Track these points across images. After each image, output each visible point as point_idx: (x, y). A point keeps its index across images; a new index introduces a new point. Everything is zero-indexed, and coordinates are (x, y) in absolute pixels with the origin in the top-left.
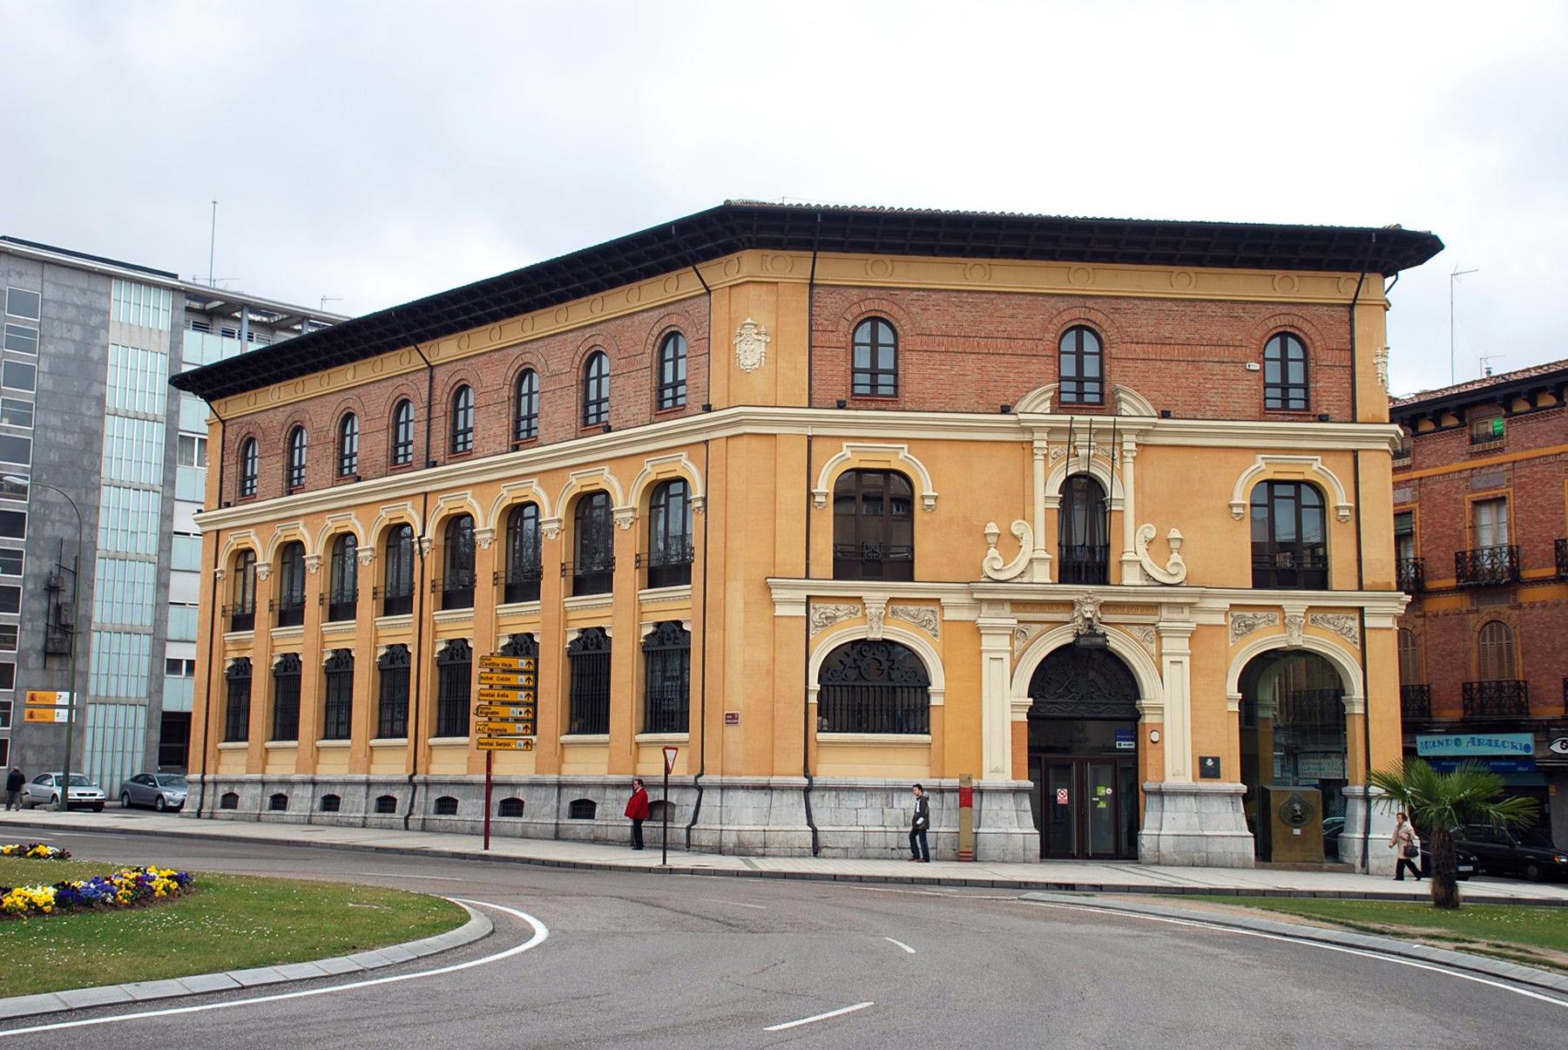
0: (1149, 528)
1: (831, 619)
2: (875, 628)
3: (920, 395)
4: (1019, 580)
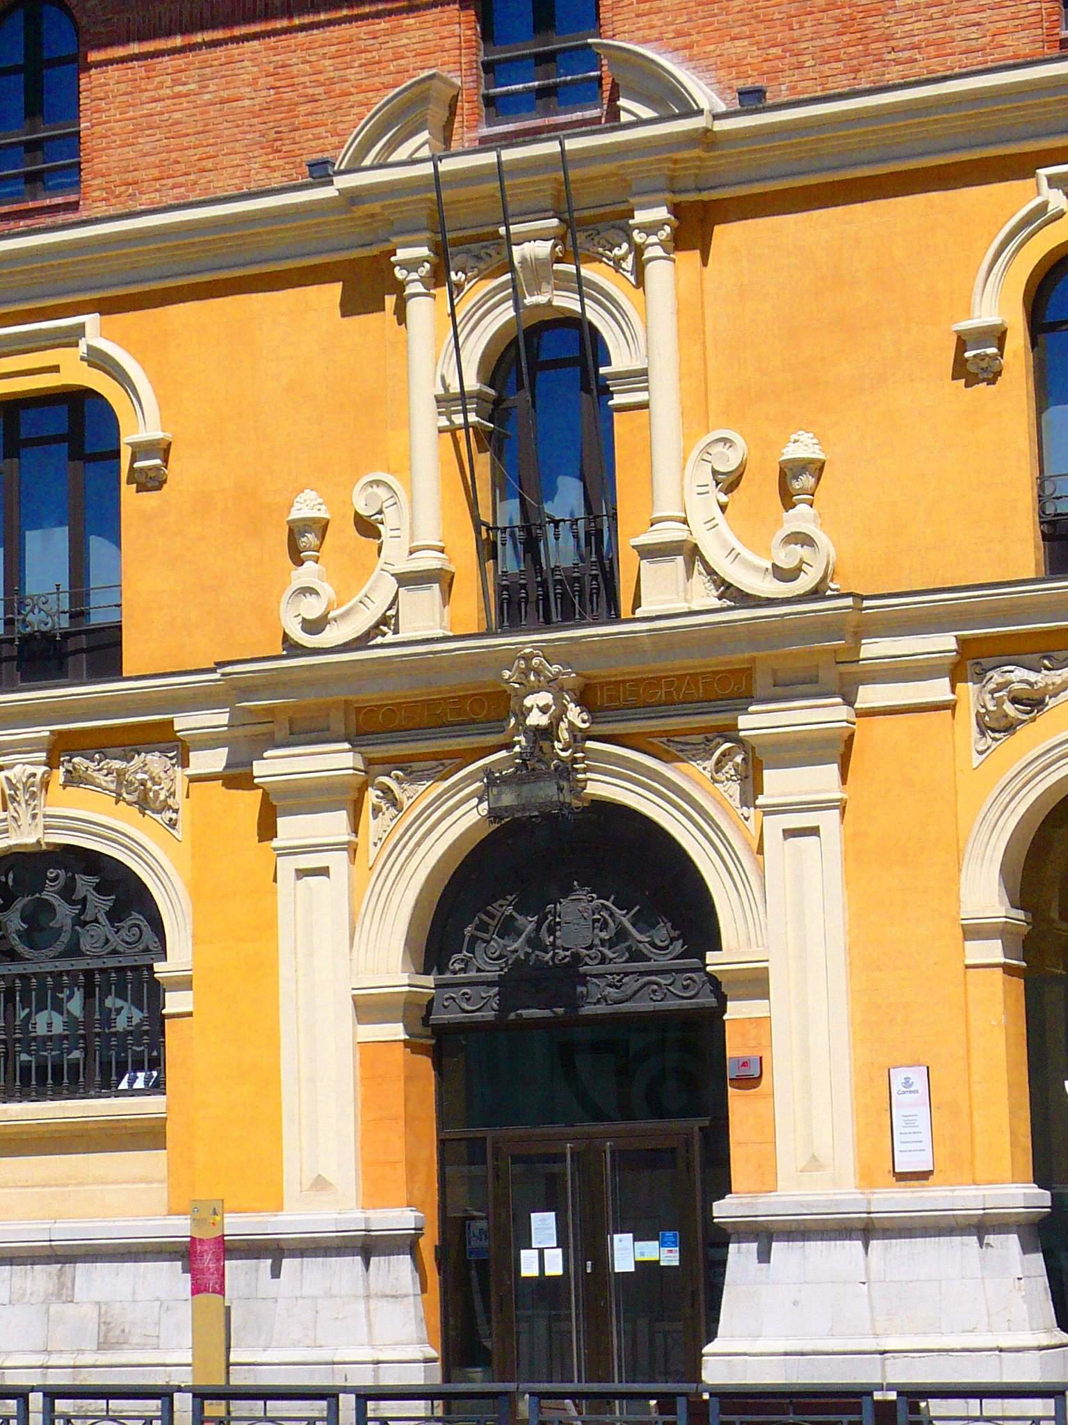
0: (725, 440)
2: (25, 819)
3: (129, 177)
4: (379, 640)
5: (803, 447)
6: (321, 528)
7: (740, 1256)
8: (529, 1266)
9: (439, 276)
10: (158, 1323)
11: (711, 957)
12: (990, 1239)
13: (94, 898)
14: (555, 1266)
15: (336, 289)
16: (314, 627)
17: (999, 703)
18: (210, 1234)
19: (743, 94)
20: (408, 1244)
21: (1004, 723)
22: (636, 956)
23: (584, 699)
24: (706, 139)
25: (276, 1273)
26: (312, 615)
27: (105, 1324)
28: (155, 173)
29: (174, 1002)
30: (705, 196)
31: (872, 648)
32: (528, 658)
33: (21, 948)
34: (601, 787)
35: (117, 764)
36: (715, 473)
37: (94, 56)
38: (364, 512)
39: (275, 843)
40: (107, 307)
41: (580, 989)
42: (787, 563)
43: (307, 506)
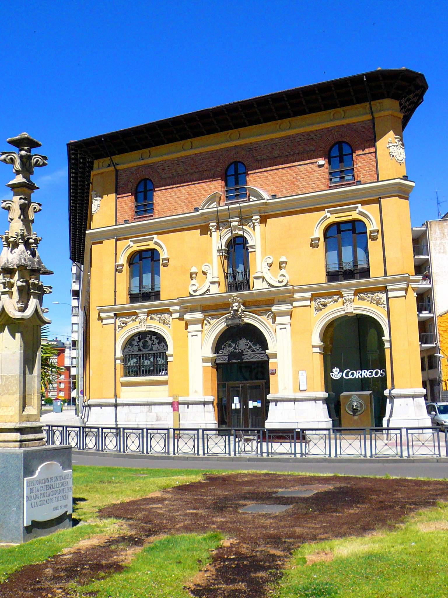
1: (126, 323)
2: (143, 326)
3: (162, 211)
4: (207, 294)
5: (283, 259)
6: (196, 273)
7: (272, 405)
8: (233, 407)
9: (217, 228)
10: (167, 416)
11: (267, 351)
12: (317, 402)
13: (155, 340)
14: (238, 407)
15: (199, 231)
16: (195, 291)
17: (319, 305)
18: (176, 400)
19: (272, 196)
20: (212, 403)
21: (319, 309)
22: (253, 351)
23: (244, 304)
24: (266, 204)
25: (188, 408)
26: (195, 289)
27: (157, 417)
28: (167, 210)
29: (169, 359)
30: (266, 214)
31: (296, 295)
32: (233, 297)
33: (142, 349)
34: (247, 320)
35: (159, 316)
36: (267, 264)
37: (156, 189)
38: (204, 271)
39: (188, 330)
40: (158, 234)
41: (243, 357)
42: (281, 280)
43: (194, 270)
